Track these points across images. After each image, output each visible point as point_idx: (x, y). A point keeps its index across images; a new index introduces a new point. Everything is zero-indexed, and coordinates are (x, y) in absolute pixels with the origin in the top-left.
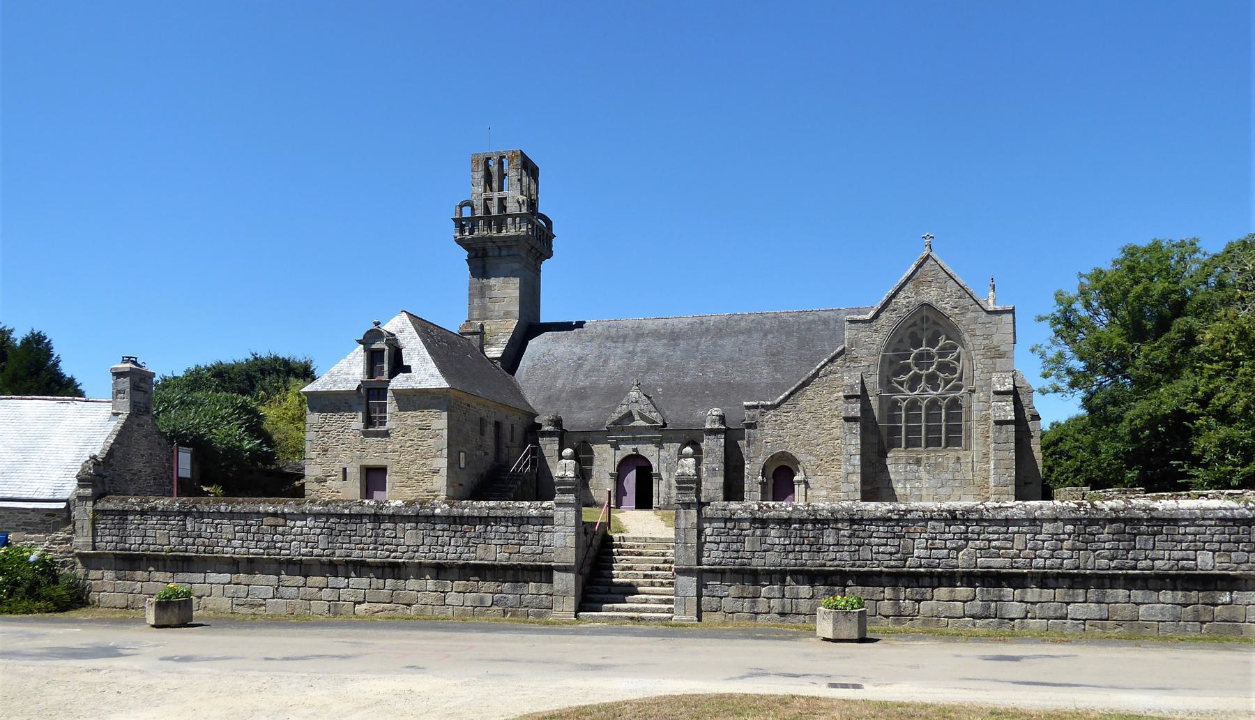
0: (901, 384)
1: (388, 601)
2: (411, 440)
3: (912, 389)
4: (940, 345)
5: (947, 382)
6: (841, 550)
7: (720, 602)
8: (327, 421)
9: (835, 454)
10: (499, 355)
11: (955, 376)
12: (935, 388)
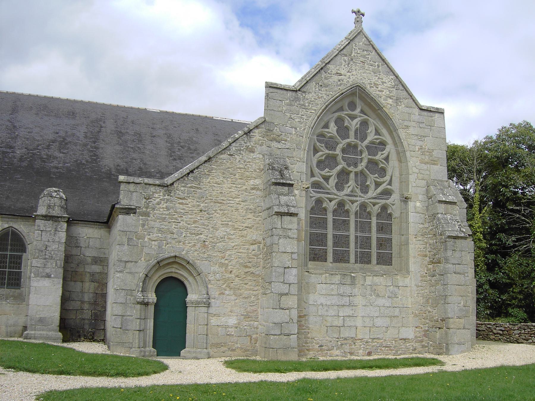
3: (339, 186)
5: (378, 185)
9: (249, 265)
11: (385, 179)
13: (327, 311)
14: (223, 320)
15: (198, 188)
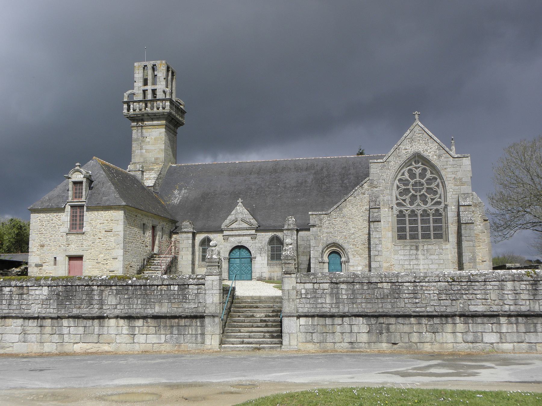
0: (404, 200)
1: (96, 342)
2: (99, 238)
3: (411, 203)
4: (427, 177)
5: (432, 200)
6: (386, 301)
7: (312, 336)
8: (44, 227)
10: (152, 185)
12: (425, 203)
13: (404, 262)
14: (355, 268)
15: (341, 213)
